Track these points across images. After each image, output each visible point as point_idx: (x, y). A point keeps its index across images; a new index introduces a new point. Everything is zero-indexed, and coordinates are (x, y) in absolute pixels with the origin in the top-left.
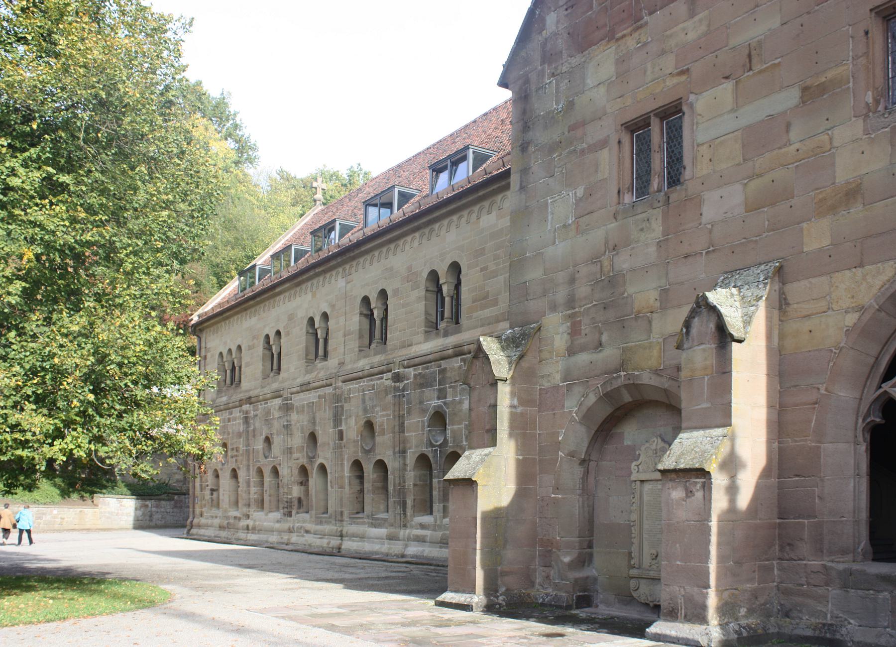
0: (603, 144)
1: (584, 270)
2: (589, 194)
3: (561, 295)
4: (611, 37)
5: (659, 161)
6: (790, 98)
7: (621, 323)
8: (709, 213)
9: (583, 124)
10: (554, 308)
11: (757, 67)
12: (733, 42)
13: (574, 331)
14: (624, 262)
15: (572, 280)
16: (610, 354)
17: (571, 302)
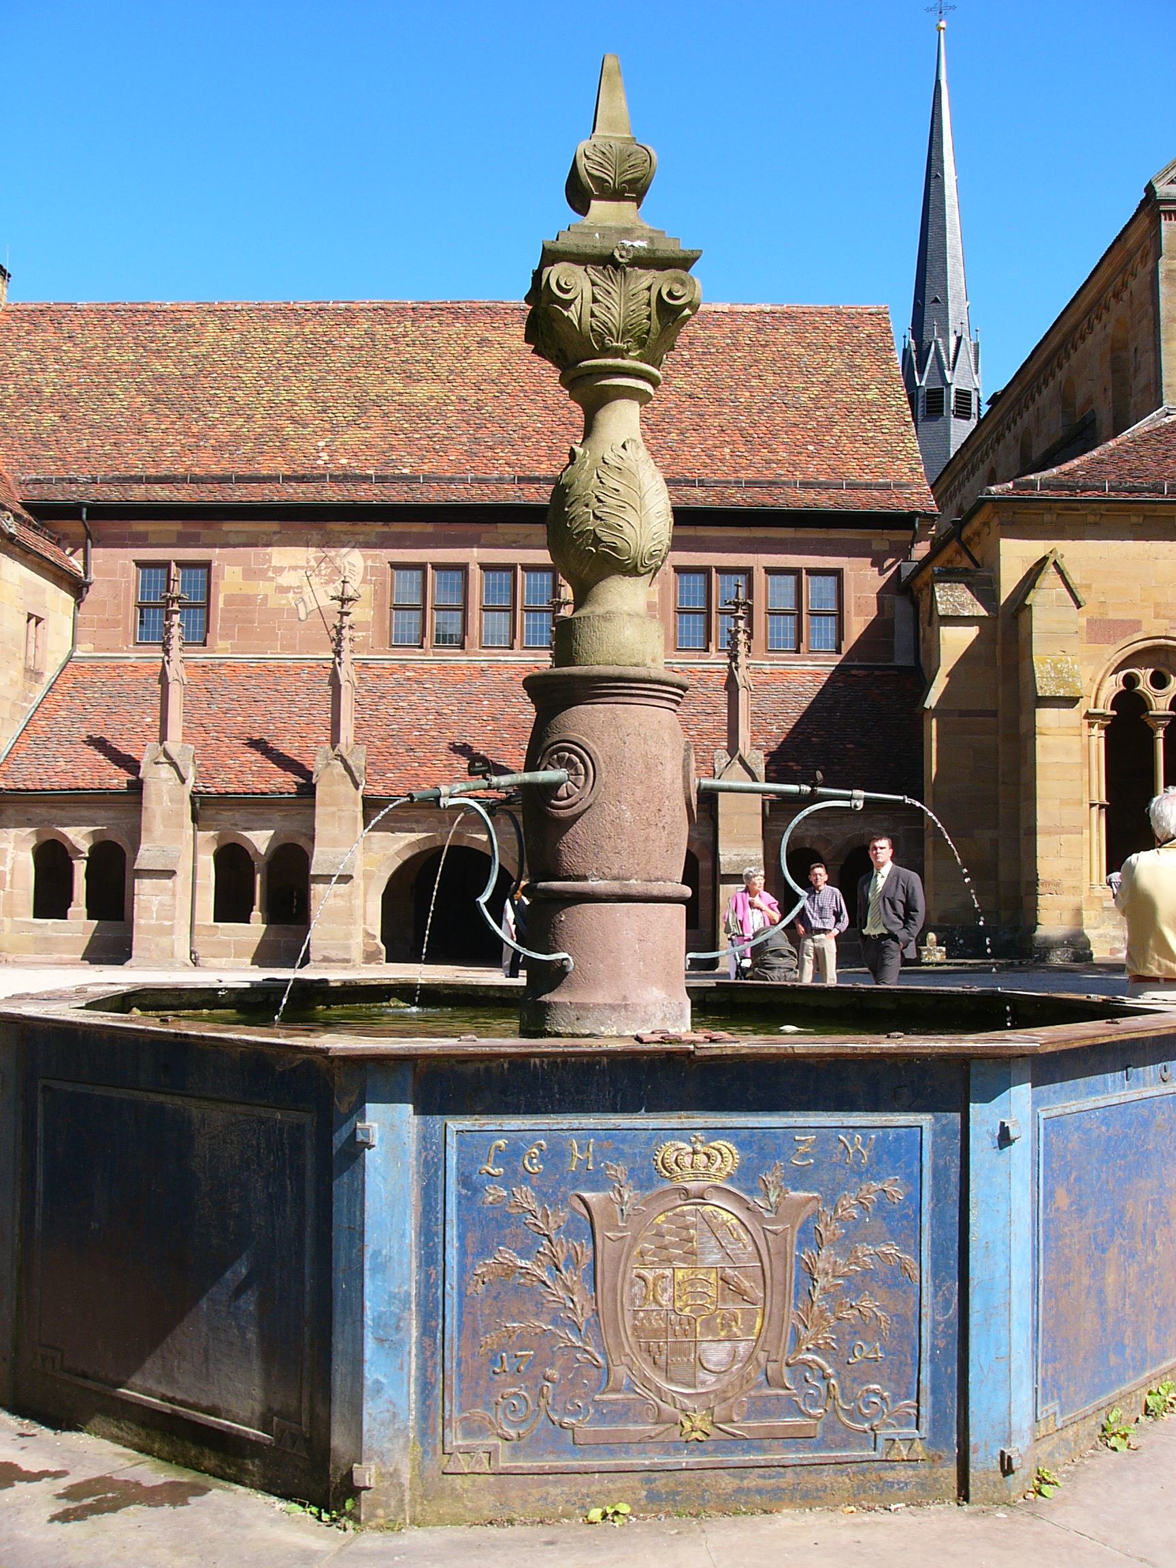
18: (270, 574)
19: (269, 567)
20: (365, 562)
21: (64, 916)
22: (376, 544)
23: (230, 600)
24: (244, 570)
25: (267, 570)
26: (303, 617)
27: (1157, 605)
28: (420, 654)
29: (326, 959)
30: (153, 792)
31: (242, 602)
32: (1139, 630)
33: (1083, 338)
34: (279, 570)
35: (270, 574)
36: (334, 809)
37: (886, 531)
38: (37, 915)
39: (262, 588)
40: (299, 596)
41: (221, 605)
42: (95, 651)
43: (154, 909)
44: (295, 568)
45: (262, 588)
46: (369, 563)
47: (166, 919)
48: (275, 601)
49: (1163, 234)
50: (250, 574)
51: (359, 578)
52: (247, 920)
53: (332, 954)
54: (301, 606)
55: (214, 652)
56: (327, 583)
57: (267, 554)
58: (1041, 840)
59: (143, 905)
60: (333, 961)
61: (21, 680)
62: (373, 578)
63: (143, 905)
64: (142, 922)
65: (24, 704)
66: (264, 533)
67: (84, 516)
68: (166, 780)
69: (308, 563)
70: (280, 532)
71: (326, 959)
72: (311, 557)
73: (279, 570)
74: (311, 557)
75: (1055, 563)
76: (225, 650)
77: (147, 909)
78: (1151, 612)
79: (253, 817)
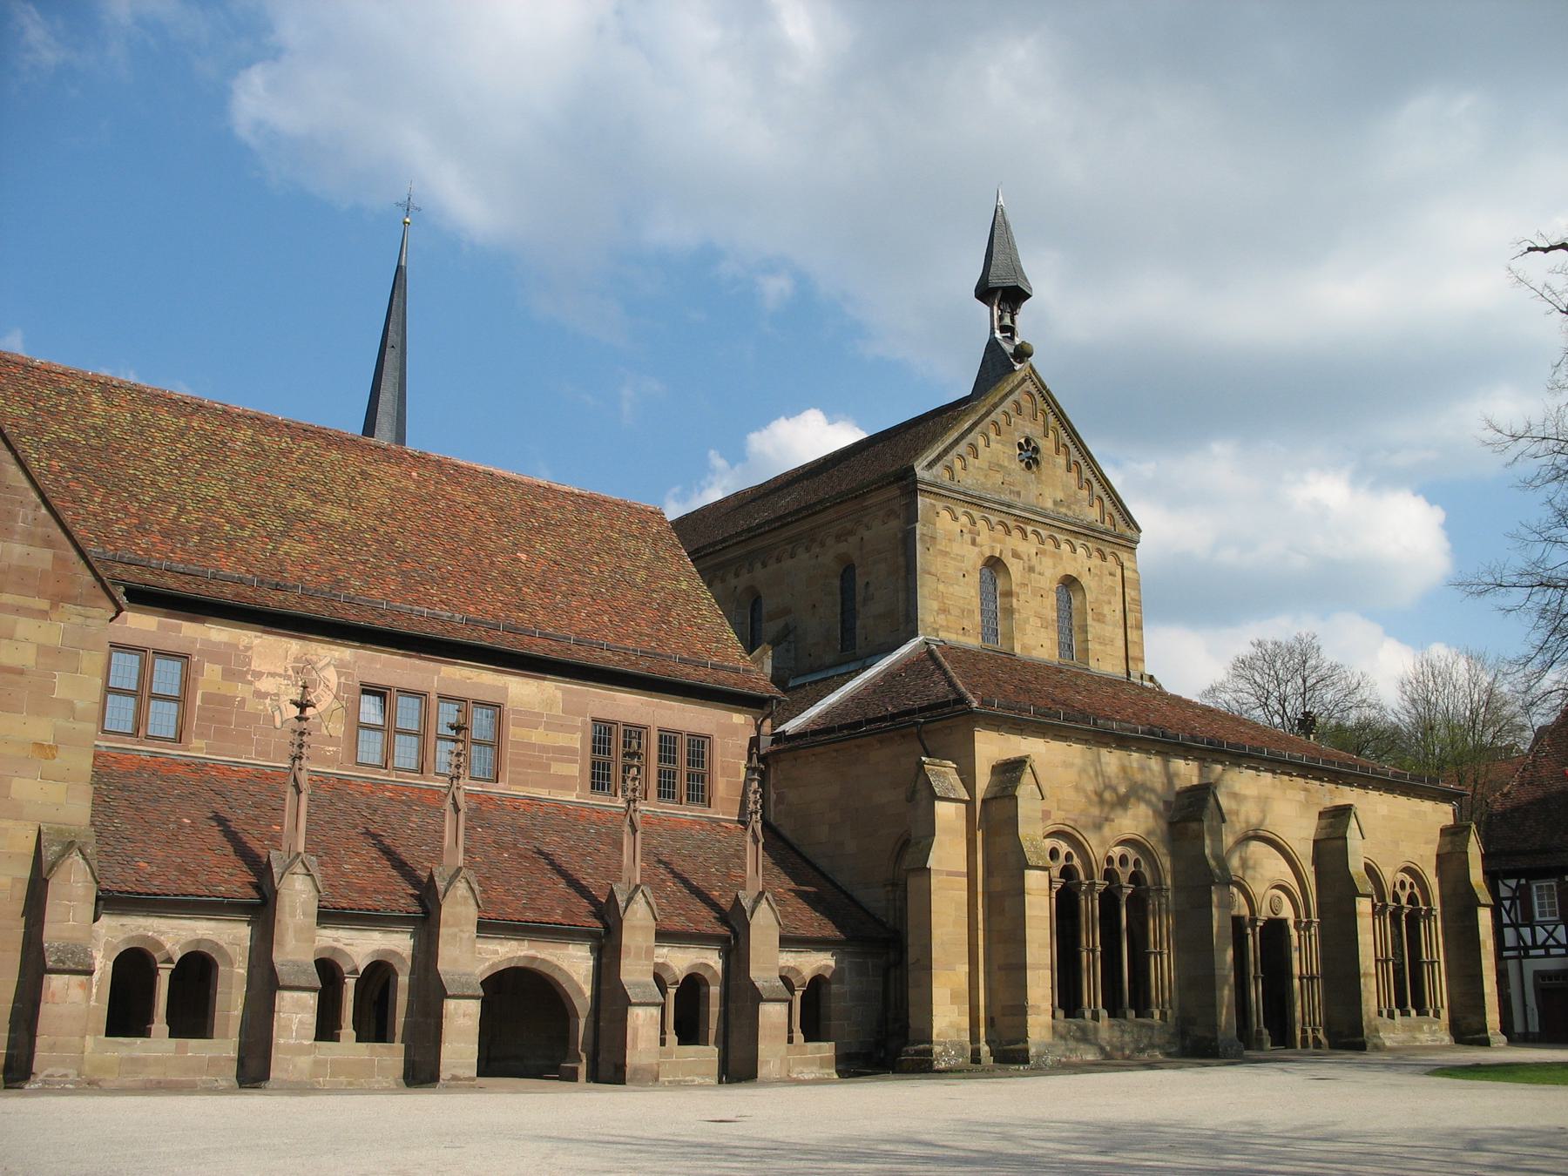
20: (339, 678)
21: (148, 1036)
22: (350, 662)
23: (207, 698)
25: (247, 672)
26: (278, 724)
27: (1059, 800)
28: (384, 775)
29: (455, 1078)
30: (287, 904)
31: (218, 702)
32: (1050, 818)
33: (779, 560)
34: (259, 675)
35: (249, 677)
36: (456, 930)
37: (745, 708)
38: (106, 1036)
41: (198, 702)
43: (294, 1028)
44: (273, 675)
45: (240, 690)
46: (343, 680)
48: (252, 705)
49: (919, 506)
52: (145, 1033)
54: (277, 713)
57: (248, 657)
58: (1029, 973)
59: (283, 1023)
60: (461, 1080)
62: (346, 695)
63: (283, 1023)
64: (282, 1041)
68: (302, 892)
69: (286, 671)
70: (261, 637)
72: (289, 666)
73: (259, 675)
74: (289, 666)
75: (1030, 766)
76: (200, 750)
77: (288, 1028)
78: (1055, 805)
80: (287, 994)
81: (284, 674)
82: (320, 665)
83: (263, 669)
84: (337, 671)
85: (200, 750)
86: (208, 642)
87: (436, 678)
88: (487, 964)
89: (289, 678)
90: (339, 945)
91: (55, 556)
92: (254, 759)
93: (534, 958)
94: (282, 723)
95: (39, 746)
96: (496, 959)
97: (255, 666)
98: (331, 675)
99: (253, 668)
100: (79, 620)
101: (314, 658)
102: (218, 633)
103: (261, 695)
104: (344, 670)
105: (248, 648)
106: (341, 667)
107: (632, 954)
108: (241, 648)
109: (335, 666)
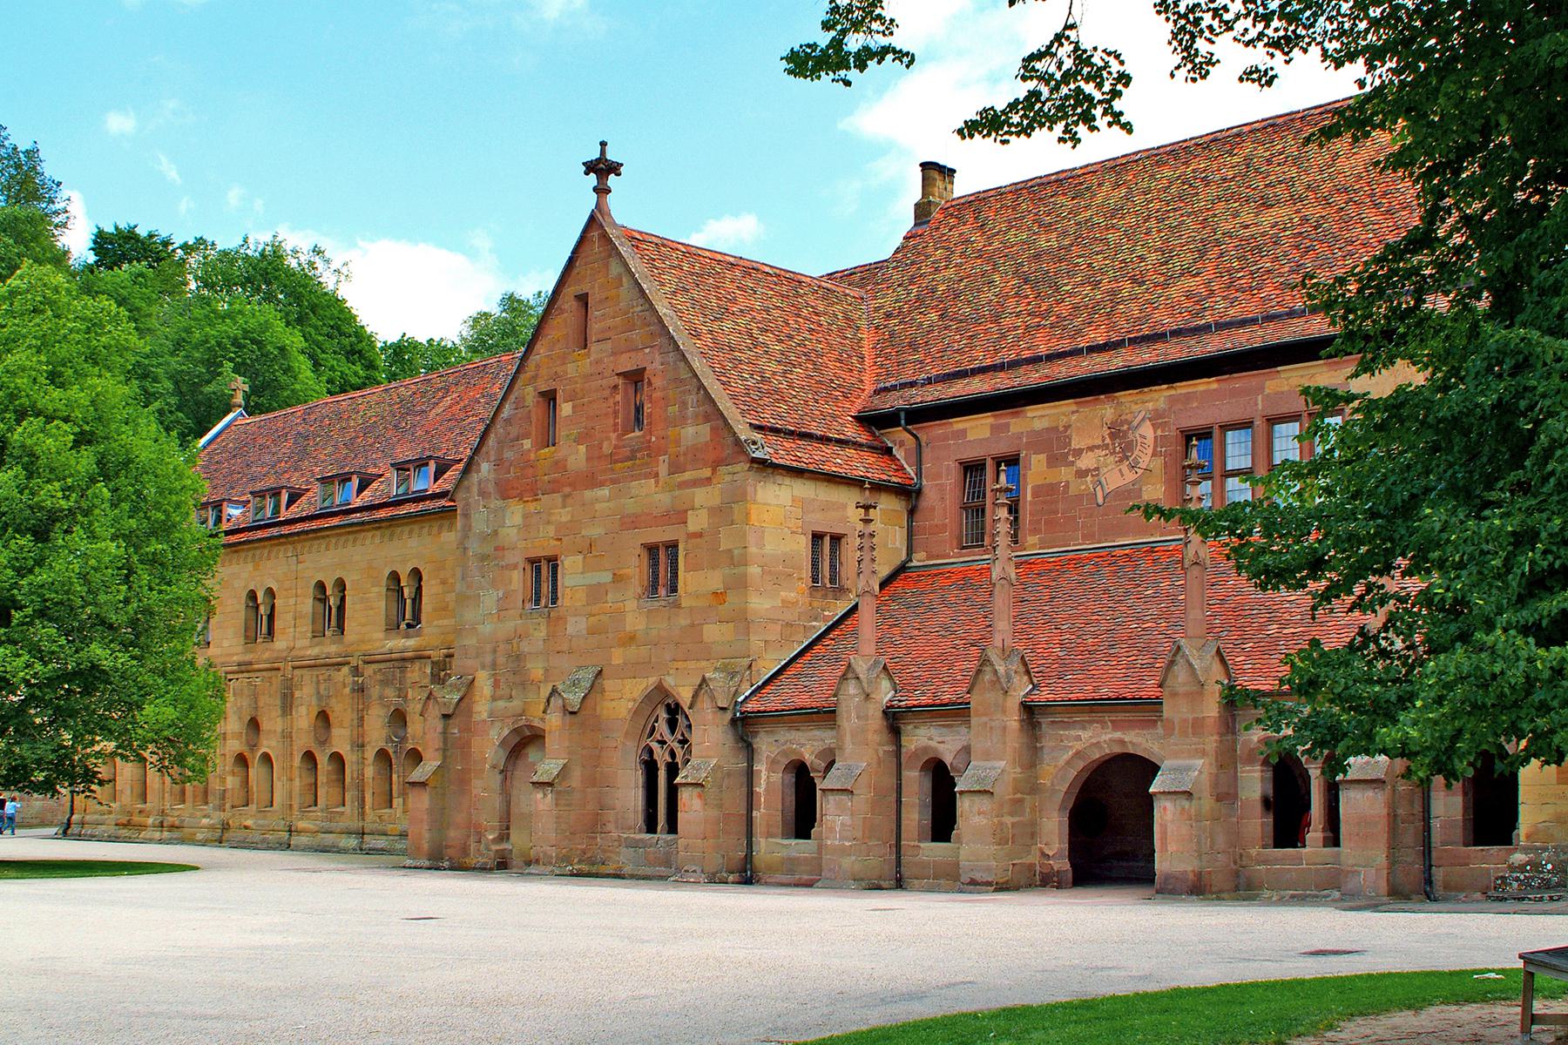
0: (515, 567)
1: (502, 646)
2: (506, 596)
3: (488, 659)
4: (520, 497)
5: (546, 588)
6: (606, 577)
7: (523, 685)
8: (570, 629)
9: (503, 549)
10: (483, 667)
11: (594, 553)
12: (584, 533)
13: (496, 685)
14: (525, 647)
15: (495, 651)
16: (516, 704)
17: (494, 665)
18: (1071, 458)
19: (1070, 450)
22: (1165, 410)
24: (1048, 458)
26: (1100, 501)
29: (973, 882)
36: (985, 719)
39: (1065, 474)
40: (1096, 478)
41: (1029, 498)
42: (928, 558)
44: (1091, 449)
46: (1159, 433)
47: (847, 839)
50: (1054, 461)
51: (1150, 451)
53: (978, 876)
55: (1025, 549)
56: (1121, 461)
60: (979, 884)
61: (804, 600)
62: (1163, 449)
64: (829, 842)
65: (814, 623)
66: (1064, 414)
67: (903, 422)
70: (1077, 411)
71: (973, 882)
76: (1033, 546)
77: (832, 830)
79: (944, 730)
80: (831, 798)
81: (1100, 443)
82: (1135, 423)
83: (1082, 445)
84: (1153, 425)
85: (1033, 546)
86: (1033, 433)
87: (1260, 397)
88: (1070, 753)
89: (1107, 447)
90: (933, 744)
91: (712, 429)
92: (1081, 544)
93: (1122, 742)
94: (1104, 498)
95: (715, 594)
96: (1078, 746)
97: (1075, 445)
98: (1147, 431)
99: (1073, 446)
100: (728, 478)
101: (1129, 417)
102: (1039, 417)
103: (1082, 474)
104: (1160, 421)
105: (1067, 427)
106: (1156, 419)
107: (1176, 732)
108: (1061, 429)
109: (1150, 419)
